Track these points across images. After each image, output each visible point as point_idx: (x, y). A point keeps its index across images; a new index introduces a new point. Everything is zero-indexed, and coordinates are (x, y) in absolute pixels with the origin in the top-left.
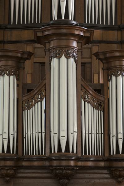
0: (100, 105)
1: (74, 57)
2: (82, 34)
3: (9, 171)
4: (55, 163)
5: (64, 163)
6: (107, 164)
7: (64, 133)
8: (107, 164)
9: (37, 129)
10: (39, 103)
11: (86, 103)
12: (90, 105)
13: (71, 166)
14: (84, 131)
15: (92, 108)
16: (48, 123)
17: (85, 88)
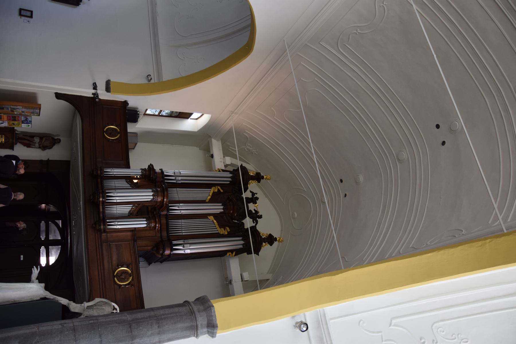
0: (131, 214)
1: (153, 198)
2: (165, 203)
3: (95, 172)
4: (101, 191)
5: (101, 195)
6: (101, 218)
7: (116, 223)
8: (101, 218)
9: (117, 185)
10: (130, 186)
11: (131, 207)
12: (130, 209)
13: (99, 198)
14: (117, 206)
15: (129, 211)
16: (121, 203)
17: (138, 206)
